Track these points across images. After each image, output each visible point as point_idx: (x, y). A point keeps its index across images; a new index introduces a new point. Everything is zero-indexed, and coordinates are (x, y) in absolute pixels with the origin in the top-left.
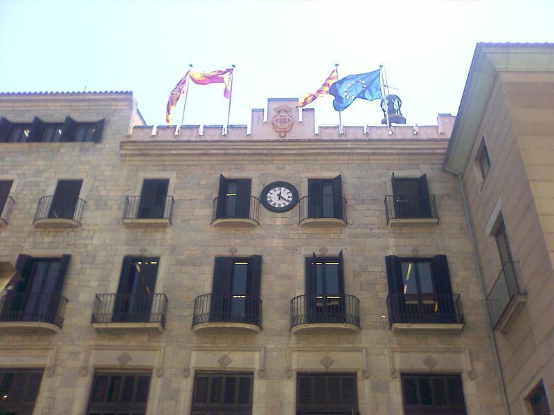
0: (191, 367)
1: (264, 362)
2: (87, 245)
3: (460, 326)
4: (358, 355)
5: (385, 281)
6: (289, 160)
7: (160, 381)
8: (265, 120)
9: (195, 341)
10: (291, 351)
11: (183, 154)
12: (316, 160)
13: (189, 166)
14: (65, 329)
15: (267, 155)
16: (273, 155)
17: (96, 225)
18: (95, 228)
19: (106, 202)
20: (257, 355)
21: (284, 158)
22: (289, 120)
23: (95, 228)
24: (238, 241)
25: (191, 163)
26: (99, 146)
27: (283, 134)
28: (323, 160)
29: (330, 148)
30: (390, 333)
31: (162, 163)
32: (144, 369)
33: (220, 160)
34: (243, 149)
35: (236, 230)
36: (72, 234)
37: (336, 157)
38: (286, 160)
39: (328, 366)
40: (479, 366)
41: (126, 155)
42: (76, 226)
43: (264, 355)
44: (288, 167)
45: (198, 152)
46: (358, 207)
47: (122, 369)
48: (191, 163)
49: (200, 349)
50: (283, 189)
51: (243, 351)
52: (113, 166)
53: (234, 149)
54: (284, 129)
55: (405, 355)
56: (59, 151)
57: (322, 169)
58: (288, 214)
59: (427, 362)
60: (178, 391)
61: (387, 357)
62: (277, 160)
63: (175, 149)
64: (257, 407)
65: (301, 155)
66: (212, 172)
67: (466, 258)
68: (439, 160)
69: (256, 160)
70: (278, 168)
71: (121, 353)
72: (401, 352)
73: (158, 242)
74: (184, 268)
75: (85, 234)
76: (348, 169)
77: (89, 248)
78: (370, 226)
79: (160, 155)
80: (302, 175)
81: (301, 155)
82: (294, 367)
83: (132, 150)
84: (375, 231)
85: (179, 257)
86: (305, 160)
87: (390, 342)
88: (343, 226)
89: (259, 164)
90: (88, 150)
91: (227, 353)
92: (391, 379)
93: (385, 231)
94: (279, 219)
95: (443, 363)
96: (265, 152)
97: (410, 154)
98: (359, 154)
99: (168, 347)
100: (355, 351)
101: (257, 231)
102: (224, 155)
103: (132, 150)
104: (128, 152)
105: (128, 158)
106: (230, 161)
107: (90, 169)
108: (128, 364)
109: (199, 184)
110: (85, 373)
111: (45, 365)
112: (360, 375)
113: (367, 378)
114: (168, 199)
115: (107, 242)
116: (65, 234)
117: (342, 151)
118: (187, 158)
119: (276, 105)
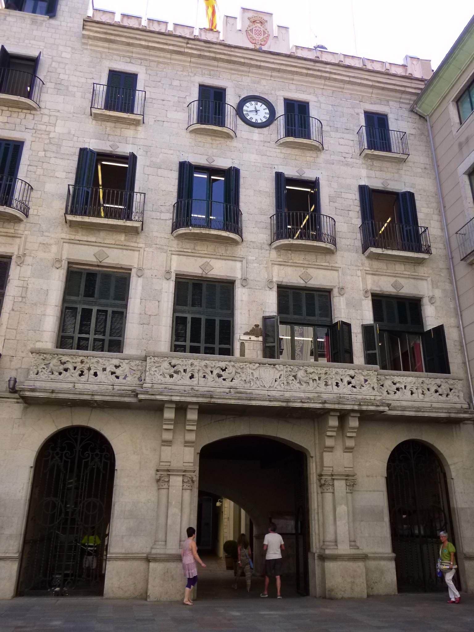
0: (172, 270)
1: (244, 271)
2: (49, 132)
3: (426, 256)
4: (335, 273)
5: (358, 209)
6: (265, 75)
7: (140, 280)
8: (239, 28)
9: (175, 246)
11: (154, 48)
12: (293, 80)
13: (159, 62)
14: (31, 218)
15: (243, 64)
16: (251, 66)
17: (59, 111)
18: (57, 114)
19: (67, 87)
20: (238, 264)
21: (260, 71)
23: (57, 114)
24: (215, 151)
25: (161, 60)
26: (53, 22)
28: (299, 81)
29: (309, 69)
30: (363, 257)
31: (131, 54)
32: (121, 268)
33: (194, 63)
34: (220, 53)
35: (212, 139)
36: (30, 117)
37: (311, 79)
38: (262, 74)
39: (306, 281)
40: (438, 293)
41: (89, 37)
42: (34, 109)
44: (264, 82)
45: (171, 48)
46: (333, 134)
47: (98, 266)
48: (161, 60)
49: (180, 253)
50: (259, 104)
51: (225, 260)
52: (73, 48)
55: (376, 278)
56: (5, 19)
57: (297, 90)
58: (265, 130)
59: (394, 286)
60: (161, 291)
61: (361, 278)
63: (145, 40)
64: (241, 313)
65: (279, 70)
66: (185, 74)
67: (428, 196)
68: (410, 100)
69: (231, 69)
71: (96, 249)
72: (372, 274)
73: (131, 140)
74: (160, 172)
75: (45, 119)
77: (52, 135)
78: (346, 155)
79: (128, 44)
80: (280, 92)
81: (279, 70)
82: (275, 279)
83: (97, 32)
84: (349, 160)
85: (154, 159)
86: (281, 78)
87: (363, 264)
88: (320, 150)
89: (233, 74)
90: (41, 24)
91: (210, 260)
92: (364, 298)
93: (358, 161)
94: (256, 134)
95: (408, 288)
96: (242, 60)
97: (383, 89)
98: (335, 80)
99: (147, 249)
101: (234, 143)
102: (200, 56)
103: (97, 32)
104: (91, 34)
105: (90, 42)
106: (205, 65)
107: (45, 47)
108: (105, 261)
109: (171, 85)
110: (60, 266)
111: (13, 253)
112: (335, 292)
114: (139, 95)
115: (73, 132)
116: (22, 115)
117: (319, 73)
118: (158, 53)
119: (250, 14)
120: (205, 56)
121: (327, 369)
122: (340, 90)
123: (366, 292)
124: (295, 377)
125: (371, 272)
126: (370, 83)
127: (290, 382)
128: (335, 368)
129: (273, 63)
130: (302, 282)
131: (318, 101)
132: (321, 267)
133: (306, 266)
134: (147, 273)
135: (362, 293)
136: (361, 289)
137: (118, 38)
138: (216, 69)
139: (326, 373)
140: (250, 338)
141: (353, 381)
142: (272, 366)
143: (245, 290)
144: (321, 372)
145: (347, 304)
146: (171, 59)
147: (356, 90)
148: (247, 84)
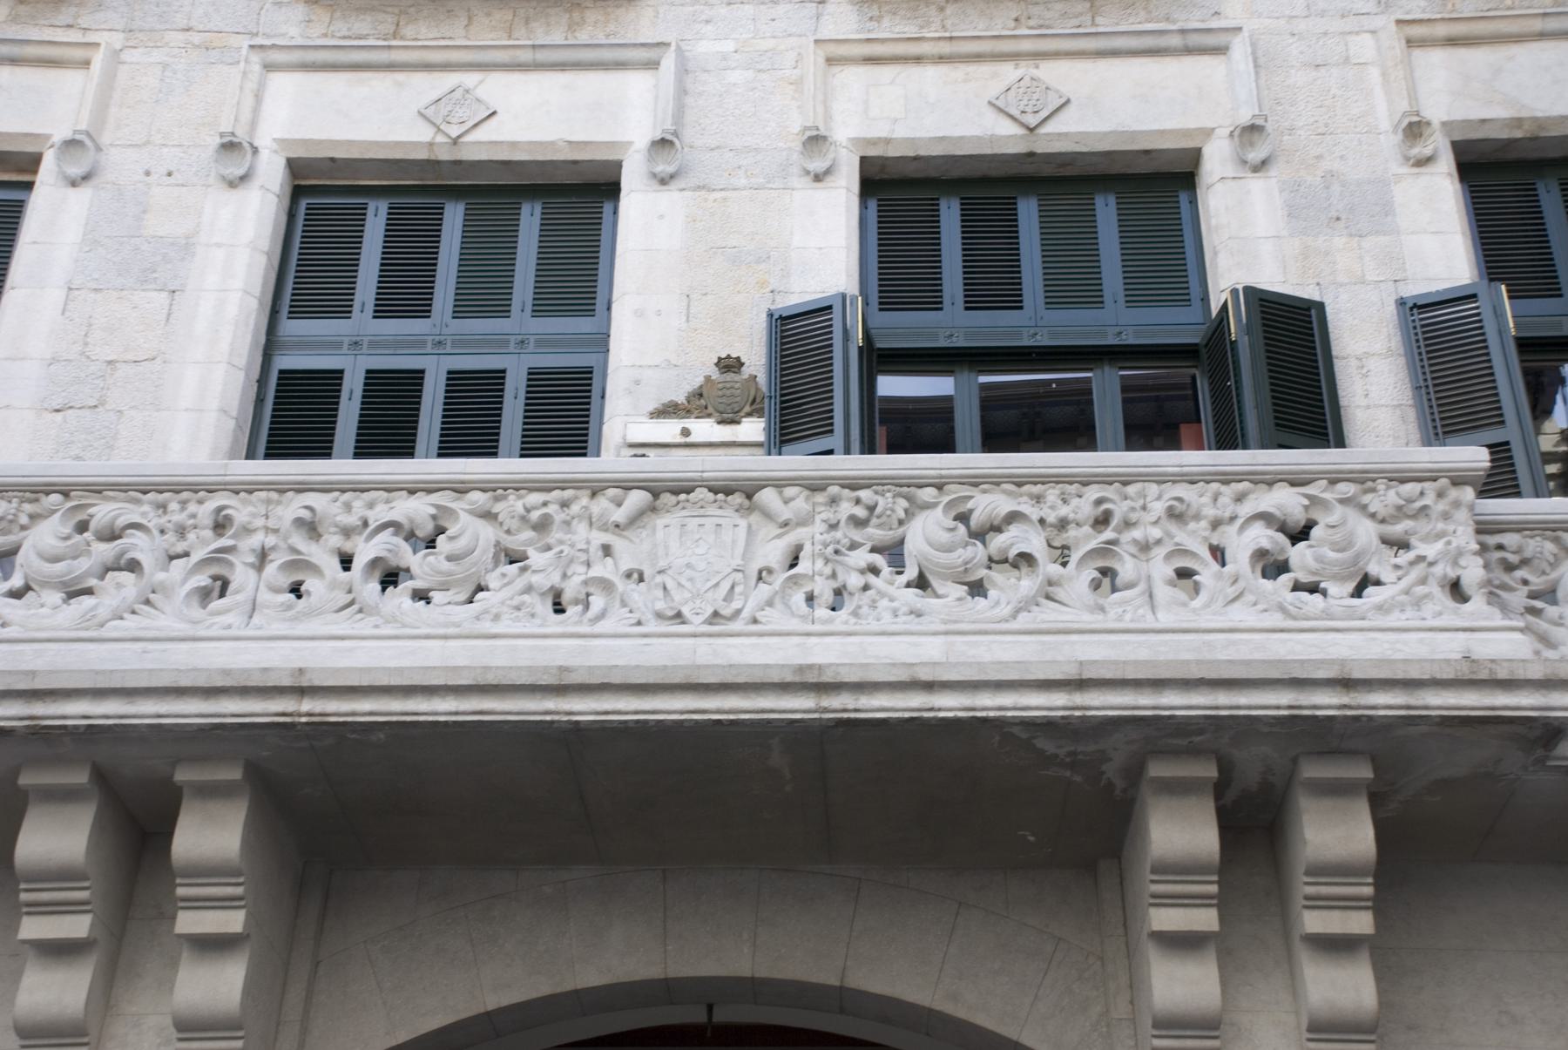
0: (264, 140)
7: (81, 197)
10: (831, 61)
20: (636, 85)
39: (1032, 120)
43: (682, 91)
61: (1374, 74)
64: (639, 313)
72: (1452, 42)
100: (1189, 51)
112: (1216, 164)
113: (1261, 166)
121: (1109, 492)
123: (1415, 130)
124: (894, 552)
125: (1442, 30)
127: (854, 581)
128: (1161, 479)
130: (1007, 128)
132: (1119, 43)
133: (1026, 46)
134: (121, 163)
135: (1390, 141)
136: (1385, 124)
139: (1102, 521)
140: (686, 432)
141: (1300, 555)
142: (737, 499)
143: (671, 200)
144: (1064, 511)
145: (1292, 213)
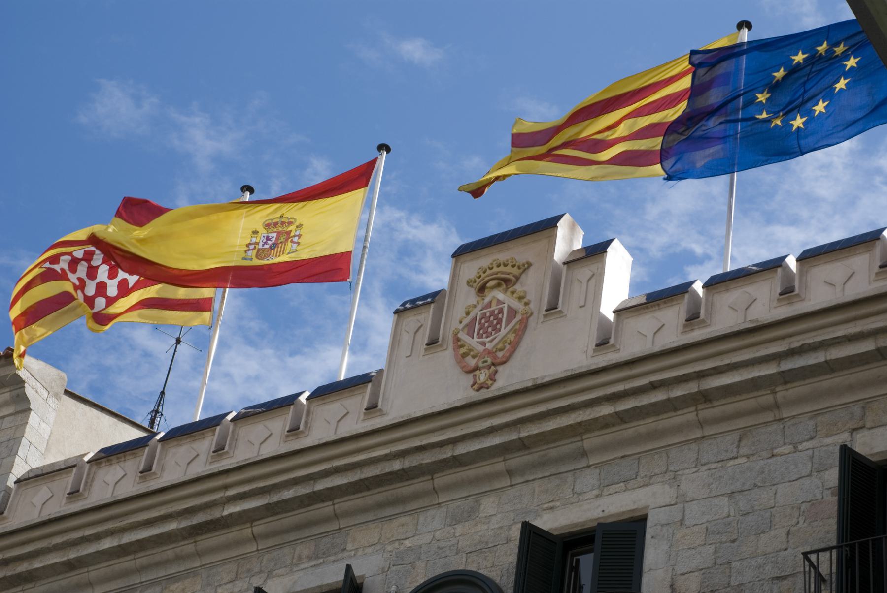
6: (496, 476)
11: (141, 546)
12: (584, 454)
21: (469, 472)
22: (513, 312)
25: (173, 570)
27: (482, 376)
28: (604, 448)
33: (266, 536)
44: (488, 506)
53: (296, 482)
54: (490, 353)
62: (448, 488)
63: (111, 533)
65: (523, 445)
69: (381, 506)
70: (456, 520)
76: (698, 463)
79: (71, 566)
96: (396, 465)
102: (271, 510)
106: (298, 527)
117: (658, 396)
120: (286, 501)
122: (769, 416)
126: (867, 346)
129: (492, 430)
131: (682, 500)
137: (37, 564)
138: (335, 526)
146: (199, 554)
147: (831, 392)
148: (429, 537)
